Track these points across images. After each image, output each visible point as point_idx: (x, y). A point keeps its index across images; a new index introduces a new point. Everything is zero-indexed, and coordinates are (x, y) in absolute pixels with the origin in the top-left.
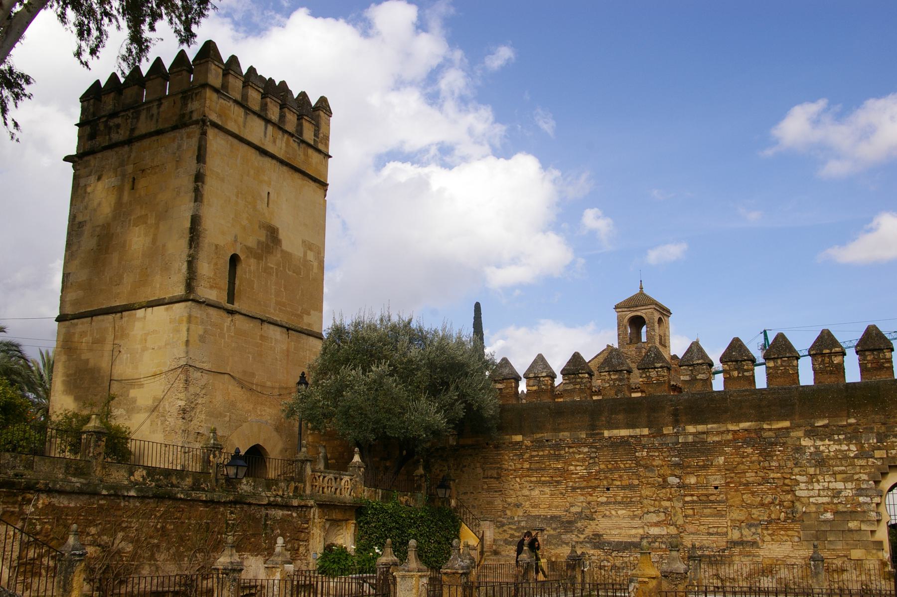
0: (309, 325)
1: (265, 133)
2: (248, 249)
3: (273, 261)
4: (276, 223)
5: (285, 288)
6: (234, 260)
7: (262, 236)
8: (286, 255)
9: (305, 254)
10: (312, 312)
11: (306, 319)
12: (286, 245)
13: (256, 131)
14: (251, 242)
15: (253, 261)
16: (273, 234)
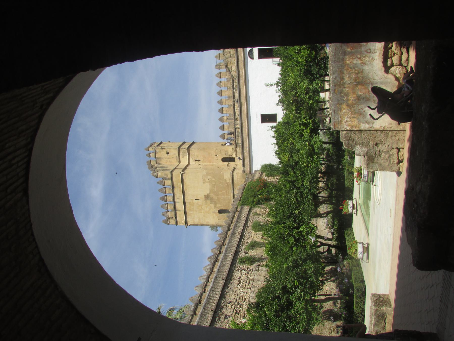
0: (229, 179)
1: (178, 202)
2: (215, 207)
3: (215, 197)
4: (203, 197)
5: (221, 191)
6: (220, 212)
7: (209, 202)
8: (211, 191)
9: (207, 182)
10: (225, 178)
11: (228, 181)
12: (208, 192)
13: (180, 206)
14: (212, 205)
15: (218, 205)
16: (207, 197)
